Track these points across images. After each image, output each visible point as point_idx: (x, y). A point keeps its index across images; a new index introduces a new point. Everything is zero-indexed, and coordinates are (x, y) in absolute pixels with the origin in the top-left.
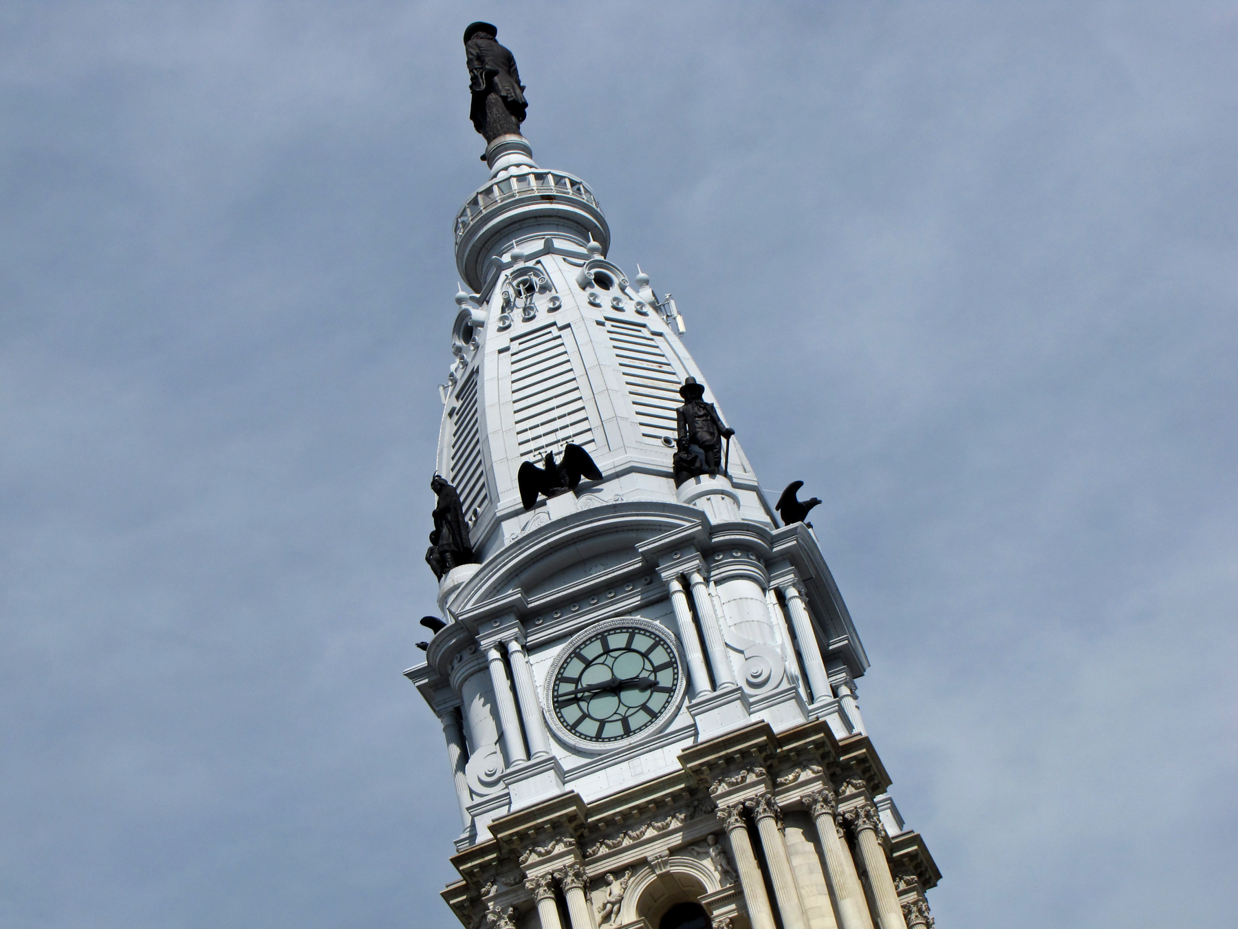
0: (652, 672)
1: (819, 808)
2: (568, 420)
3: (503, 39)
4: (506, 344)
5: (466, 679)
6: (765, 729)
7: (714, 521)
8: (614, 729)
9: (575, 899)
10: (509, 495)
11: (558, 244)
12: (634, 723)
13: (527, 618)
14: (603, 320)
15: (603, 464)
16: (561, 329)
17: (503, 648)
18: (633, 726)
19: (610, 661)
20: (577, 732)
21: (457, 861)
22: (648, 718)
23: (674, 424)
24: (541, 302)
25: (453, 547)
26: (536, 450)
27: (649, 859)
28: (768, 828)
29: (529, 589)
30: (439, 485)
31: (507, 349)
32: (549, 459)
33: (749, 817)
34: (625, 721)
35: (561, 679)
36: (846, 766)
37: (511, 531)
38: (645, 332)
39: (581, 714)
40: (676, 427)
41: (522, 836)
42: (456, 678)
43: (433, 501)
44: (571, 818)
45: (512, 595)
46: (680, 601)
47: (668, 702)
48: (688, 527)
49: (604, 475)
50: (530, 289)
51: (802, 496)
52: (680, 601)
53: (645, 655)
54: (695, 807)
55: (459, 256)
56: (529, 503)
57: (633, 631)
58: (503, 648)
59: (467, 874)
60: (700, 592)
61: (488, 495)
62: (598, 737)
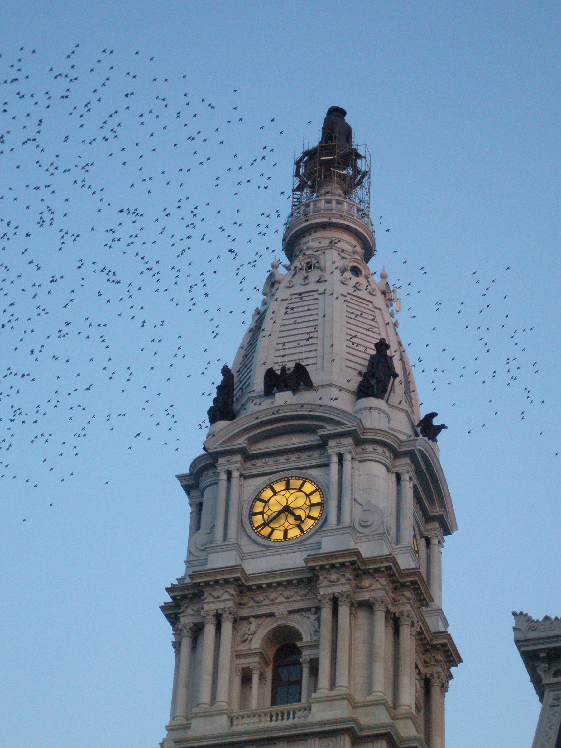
0: (309, 506)
3: (348, 119)
6: (358, 553)
7: (367, 425)
9: (227, 627)
13: (248, 457)
14: (346, 294)
15: (315, 378)
17: (229, 474)
19: (288, 495)
21: (169, 590)
23: (366, 363)
26: (281, 362)
27: (276, 614)
28: (344, 611)
30: (226, 371)
32: (284, 369)
33: (335, 601)
36: (403, 585)
37: (252, 408)
38: (370, 306)
41: (207, 584)
44: (237, 579)
45: (241, 442)
46: (334, 467)
48: (350, 426)
49: (314, 385)
51: (436, 422)
52: (334, 467)
53: (308, 496)
55: (284, 240)
56: (268, 392)
58: (229, 474)
59: (174, 598)
60: (347, 464)
61: (247, 383)
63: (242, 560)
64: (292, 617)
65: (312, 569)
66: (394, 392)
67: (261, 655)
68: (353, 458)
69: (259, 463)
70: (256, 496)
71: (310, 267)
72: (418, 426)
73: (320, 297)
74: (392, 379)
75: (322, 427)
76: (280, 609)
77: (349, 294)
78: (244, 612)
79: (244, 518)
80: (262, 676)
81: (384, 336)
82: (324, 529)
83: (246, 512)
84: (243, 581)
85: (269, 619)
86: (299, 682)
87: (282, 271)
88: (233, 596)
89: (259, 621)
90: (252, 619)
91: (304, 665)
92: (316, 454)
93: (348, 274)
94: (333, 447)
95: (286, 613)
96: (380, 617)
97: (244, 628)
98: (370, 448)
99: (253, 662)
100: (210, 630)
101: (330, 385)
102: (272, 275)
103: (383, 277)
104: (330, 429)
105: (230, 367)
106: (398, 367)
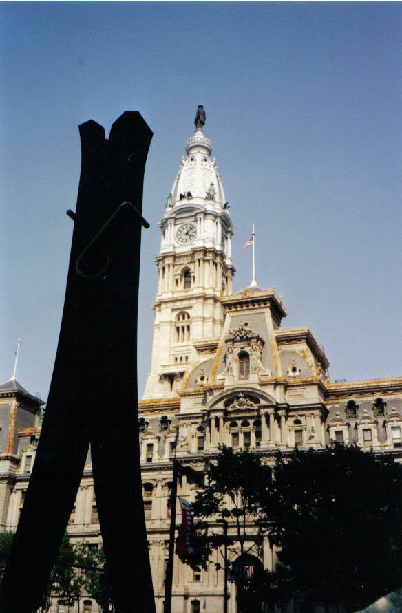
9: (171, 267)
10: (178, 198)
11: (201, 151)
13: (176, 219)
24: (193, 162)
28: (201, 262)
29: (177, 215)
45: (174, 215)
48: (203, 210)
52: (198, 222)
56: (181, 199)
67: (181, 275)
71: (192, 160)
76: (185, 262)
78: (176, 263)
80: (181, 280)
86: (190, 282)
94: (198, 217)
96: (211, 263)
97: (176, 267)
99: (179, 277)
100: (167, 269)
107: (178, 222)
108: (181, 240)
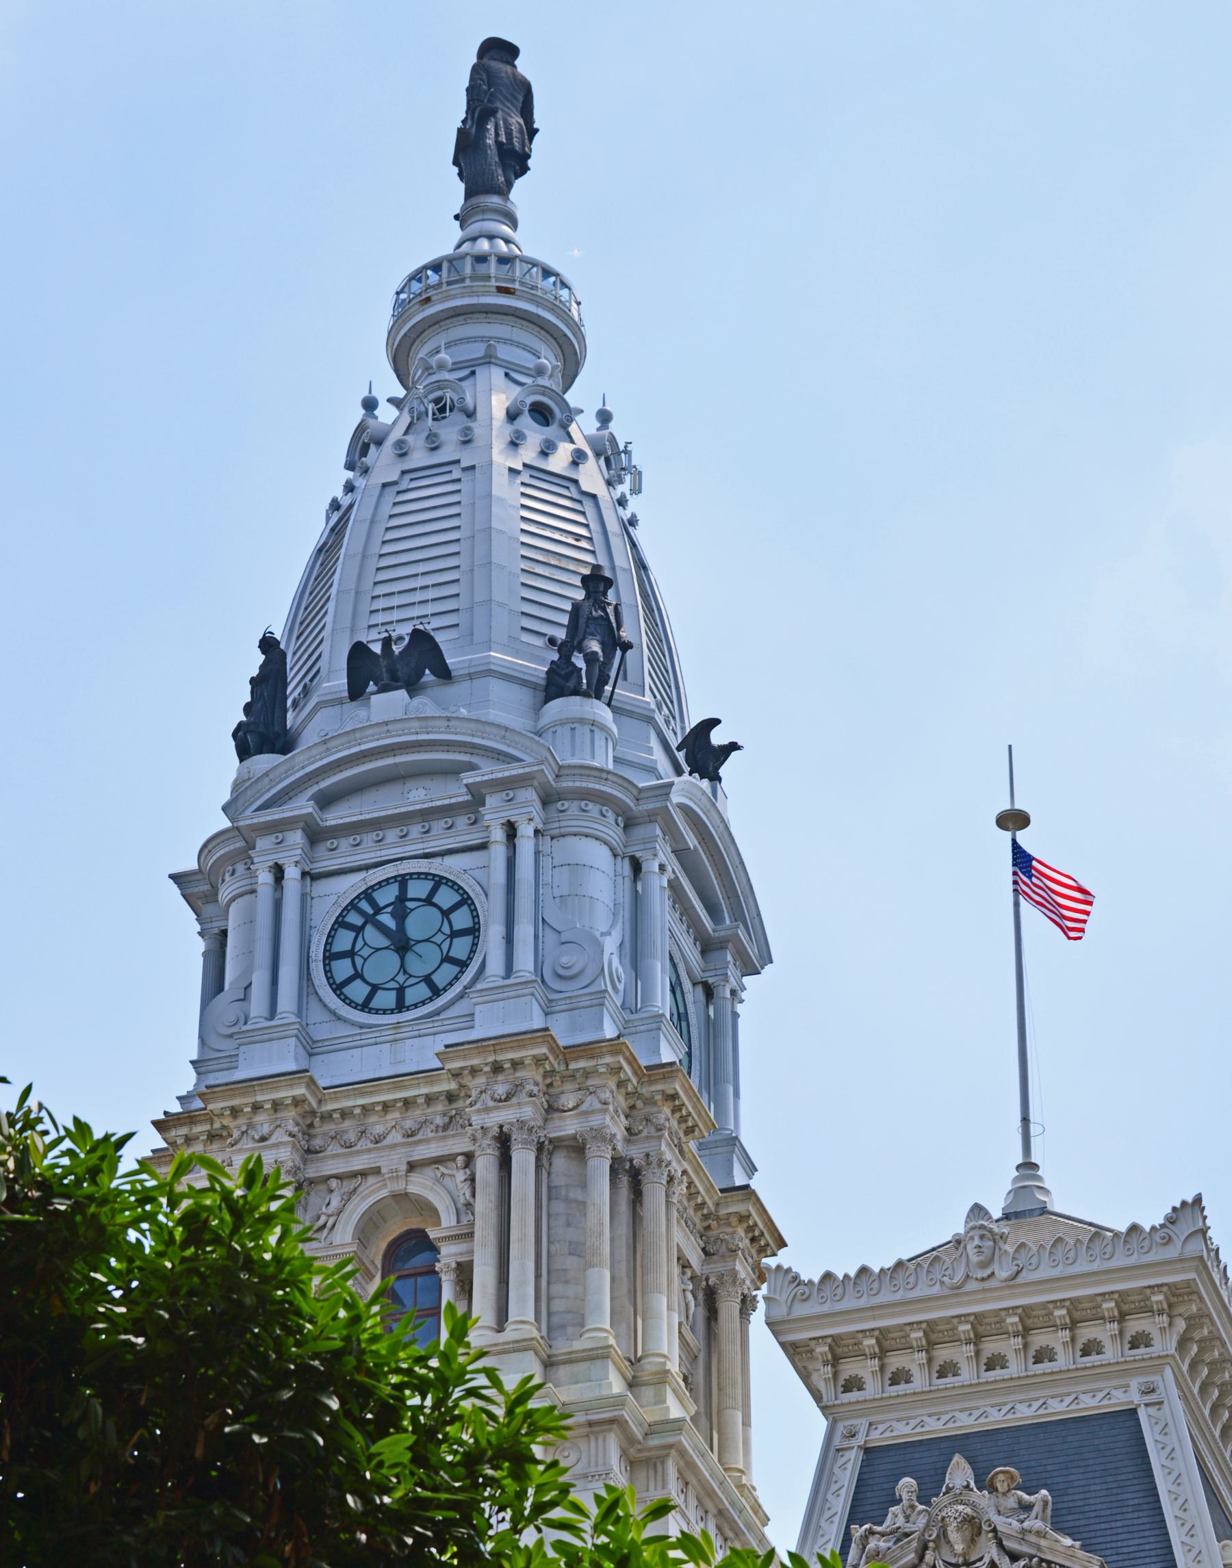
0: (449, 936)
1: (592, 1149)
2: (431, 594)
3: (523, 66)
4: (394, 477)
5: (233, 899)
8: (386, 999)
12: (411, 996)
13: (315, 836)
14: (520, 468)
16: (465, 469)
18: (409, 1000)
20: (342, 993)
22: (428, 993)
23: (565, 619)
24: (449, 432)
25: (261, 729)
26: (383, 624)
27: (384, 1170)
29: (325, 801)
30: (268, 644)
31: (395, 483)
33: (504, 1142)
34: (401, 992)
35: (340, 923)
39: (353, 972)
40: (566, 623)
42: (225, 894)
43: (255, 660)
45: (303, 805)
46: (498, 852)
47: (457, 978)
49: (454, 674)
50: (442, 409)
51: (718, 737)
53: (446, 914)
54: (451, 1118)
56: (356, 692)
57: (439, 882)
62: (365, 1006)
63: (311, 1055)
64: (415, 1177)
65: (456, 1075)
66: (625, 679)
68: (537, 832)
69: (345, 844)
70: (338, 918)
72: (679, 749)
73: (465, 477)
74: (619, 653)
75: (472, 767)
77: (525, 465)
79: (312, 966)
81: (602, 561)
82: (479, 986)
83: (317, 952)
84: (314, 1104)
85: (371, 1180)
87: (386, 414)
88: (291, 1135)
89: (349, 1185)
90: (334, 1183)
91: (444, 1277)
92: (462, 822)
93: (526, 422)
94: (494, 812)
95: (404, 1167)
96: (600, 1167)
98: (572, 807)
101: (489, 673)
102: (361, 429)
103: (604, 417)
104: (489, 771)
105: (278, 636)
106: (633, 629)
107: (343, 854)
108: (358, 991)
